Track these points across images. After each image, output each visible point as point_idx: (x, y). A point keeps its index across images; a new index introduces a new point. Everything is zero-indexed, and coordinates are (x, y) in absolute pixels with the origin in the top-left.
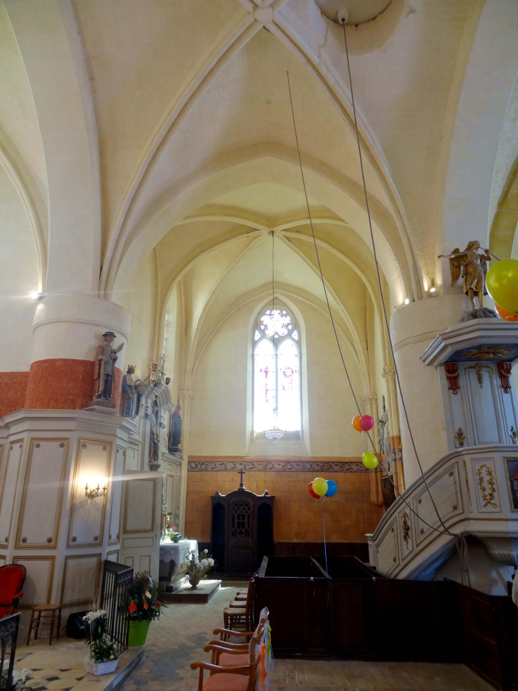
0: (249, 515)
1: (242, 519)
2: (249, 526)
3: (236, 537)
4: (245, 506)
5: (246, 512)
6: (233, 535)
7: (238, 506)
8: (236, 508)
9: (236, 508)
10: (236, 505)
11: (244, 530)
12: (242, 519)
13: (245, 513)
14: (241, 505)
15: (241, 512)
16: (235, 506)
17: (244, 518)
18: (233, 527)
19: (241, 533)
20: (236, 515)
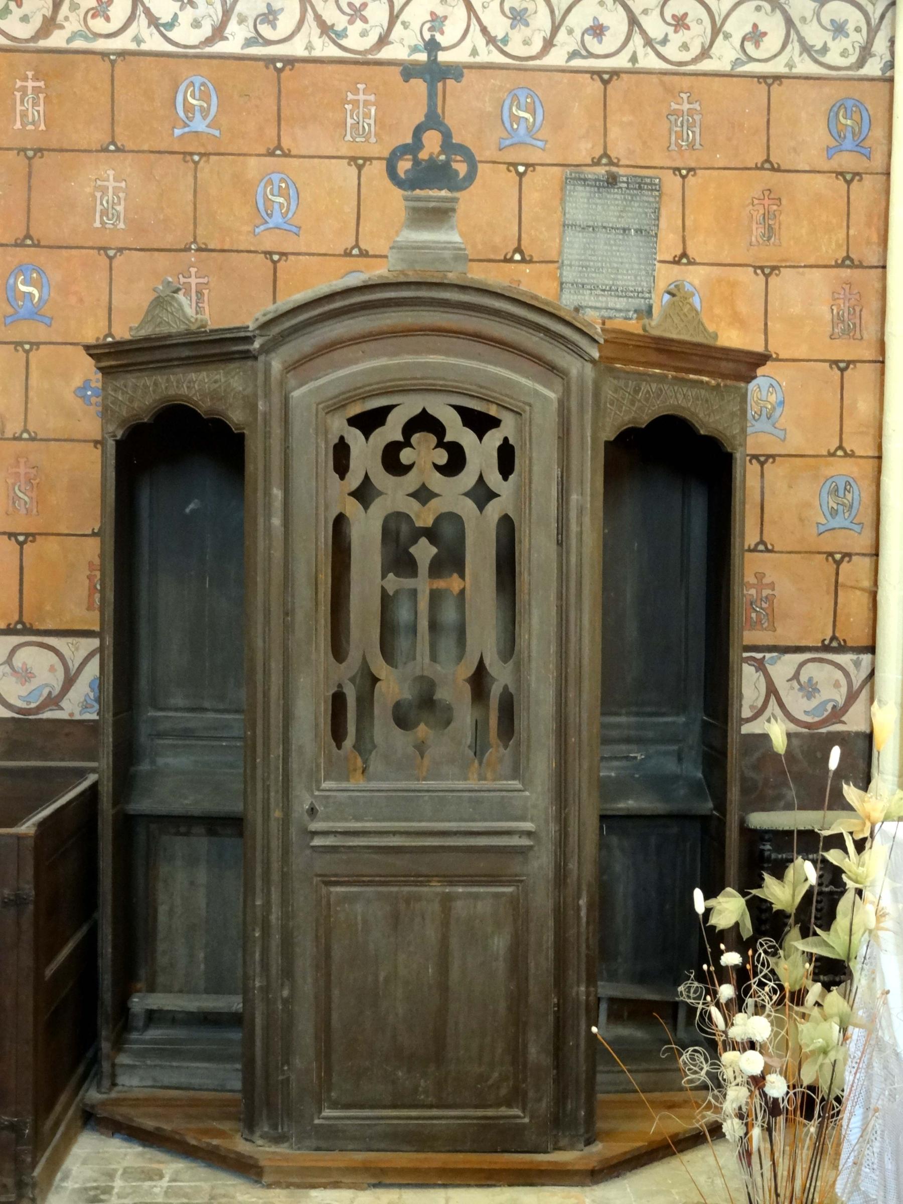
0: (507, 530)
1: (437, 568)
2: (510, 646)
3: (363, 747)
4: (466, 437)
5: (482, 494)
6: (338, 733)
7: (392, 431)
8: (365, 452)
9: (365, 452)
10: (368, 422)
11: (454, 689)
12: (437, 568)
13: (467, 508)
14: (424, 422)
15: (423, 495)
16: (355, 437)
17: (451, 560)
18: (338, 650)
19: (424, 706)
20: (366, 528)
